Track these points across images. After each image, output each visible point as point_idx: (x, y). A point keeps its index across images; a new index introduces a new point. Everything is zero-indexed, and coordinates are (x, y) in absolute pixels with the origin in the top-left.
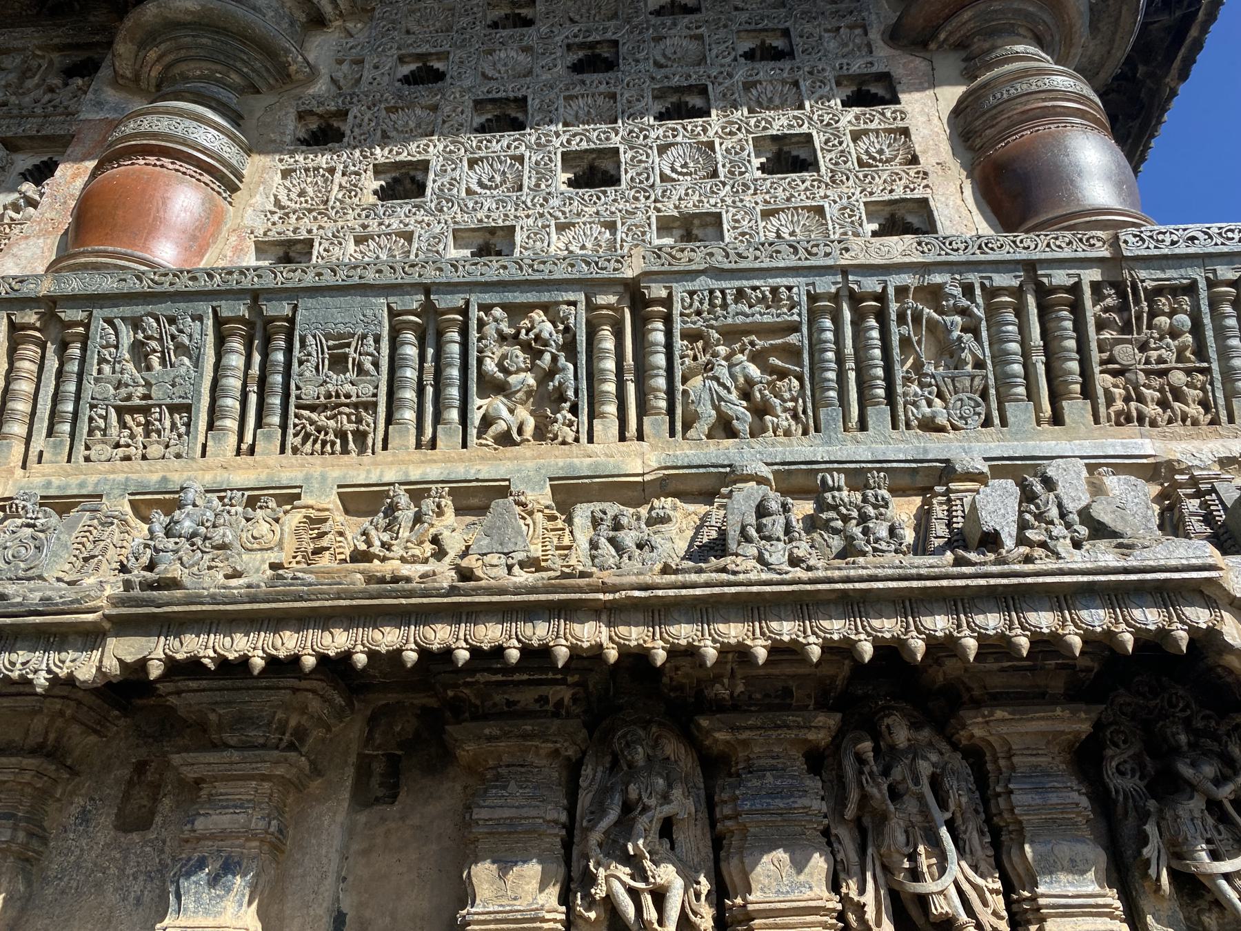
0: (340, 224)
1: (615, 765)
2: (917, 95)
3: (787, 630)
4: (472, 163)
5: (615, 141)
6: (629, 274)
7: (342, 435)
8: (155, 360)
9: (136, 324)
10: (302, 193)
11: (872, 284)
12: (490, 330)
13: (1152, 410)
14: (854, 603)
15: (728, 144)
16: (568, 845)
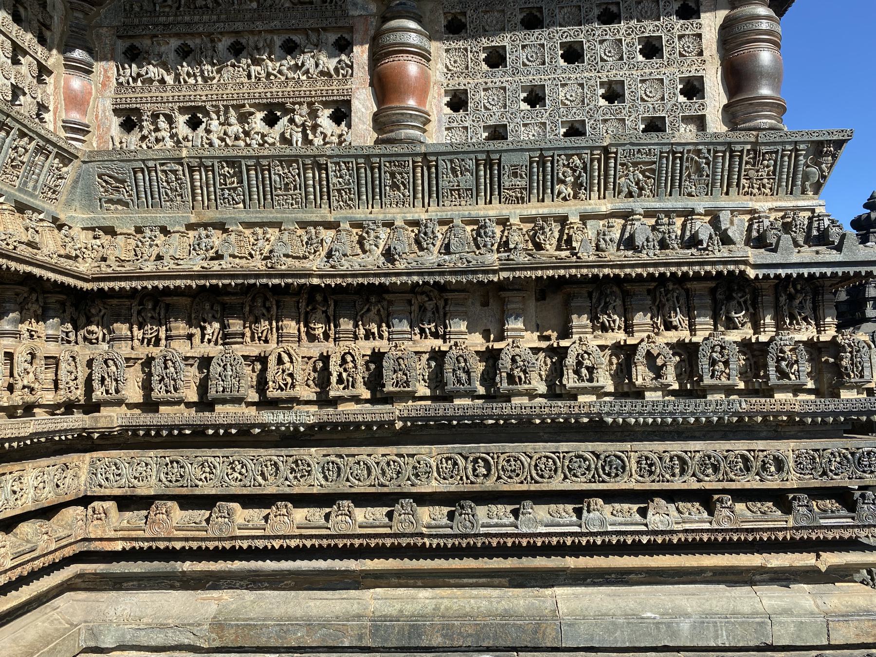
0: (476, 81)
1: (601, 294)
2: (708, 14)
3: (651, 270)
4: (524, 47)
5: (581, 38)
6: (605, 144)
7: (517, 198)
8: (459, 173)
9: (451, 161)
10: (455, 62)
11: (680, 149)
12: (561, 163)
13: (755, 191)
14: (667, 265)
15: (628, 40)
16: (591, 310)
